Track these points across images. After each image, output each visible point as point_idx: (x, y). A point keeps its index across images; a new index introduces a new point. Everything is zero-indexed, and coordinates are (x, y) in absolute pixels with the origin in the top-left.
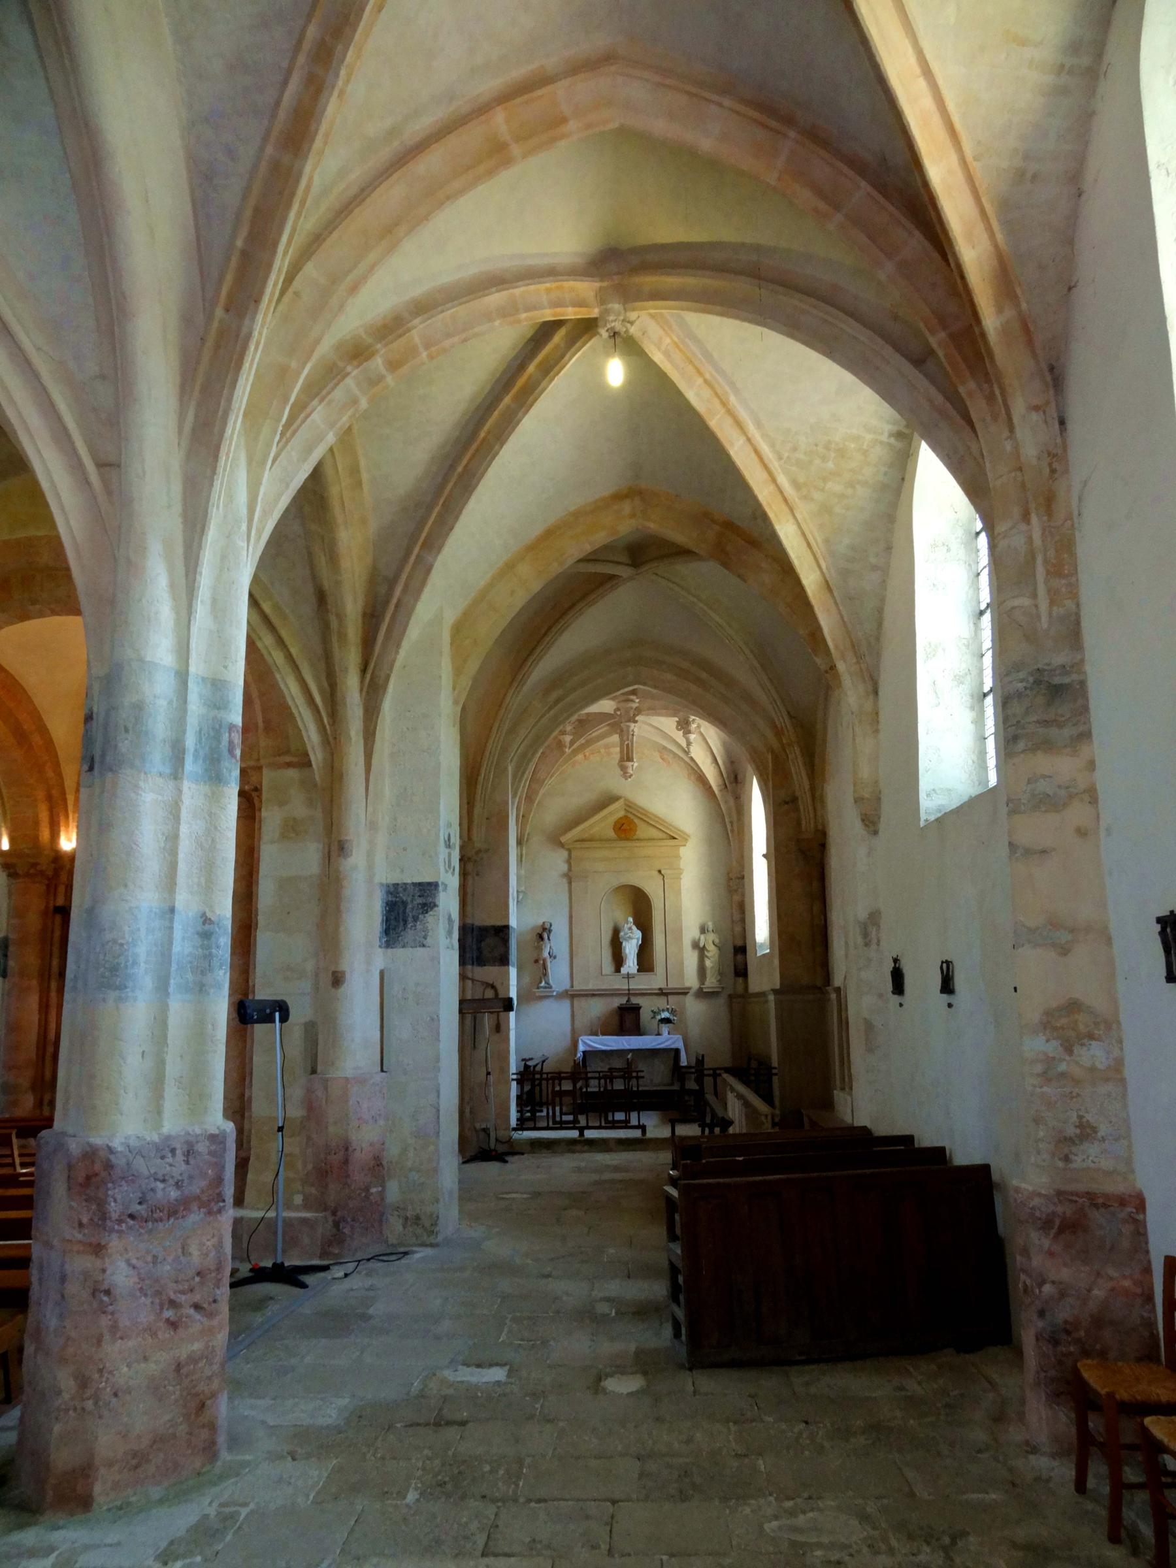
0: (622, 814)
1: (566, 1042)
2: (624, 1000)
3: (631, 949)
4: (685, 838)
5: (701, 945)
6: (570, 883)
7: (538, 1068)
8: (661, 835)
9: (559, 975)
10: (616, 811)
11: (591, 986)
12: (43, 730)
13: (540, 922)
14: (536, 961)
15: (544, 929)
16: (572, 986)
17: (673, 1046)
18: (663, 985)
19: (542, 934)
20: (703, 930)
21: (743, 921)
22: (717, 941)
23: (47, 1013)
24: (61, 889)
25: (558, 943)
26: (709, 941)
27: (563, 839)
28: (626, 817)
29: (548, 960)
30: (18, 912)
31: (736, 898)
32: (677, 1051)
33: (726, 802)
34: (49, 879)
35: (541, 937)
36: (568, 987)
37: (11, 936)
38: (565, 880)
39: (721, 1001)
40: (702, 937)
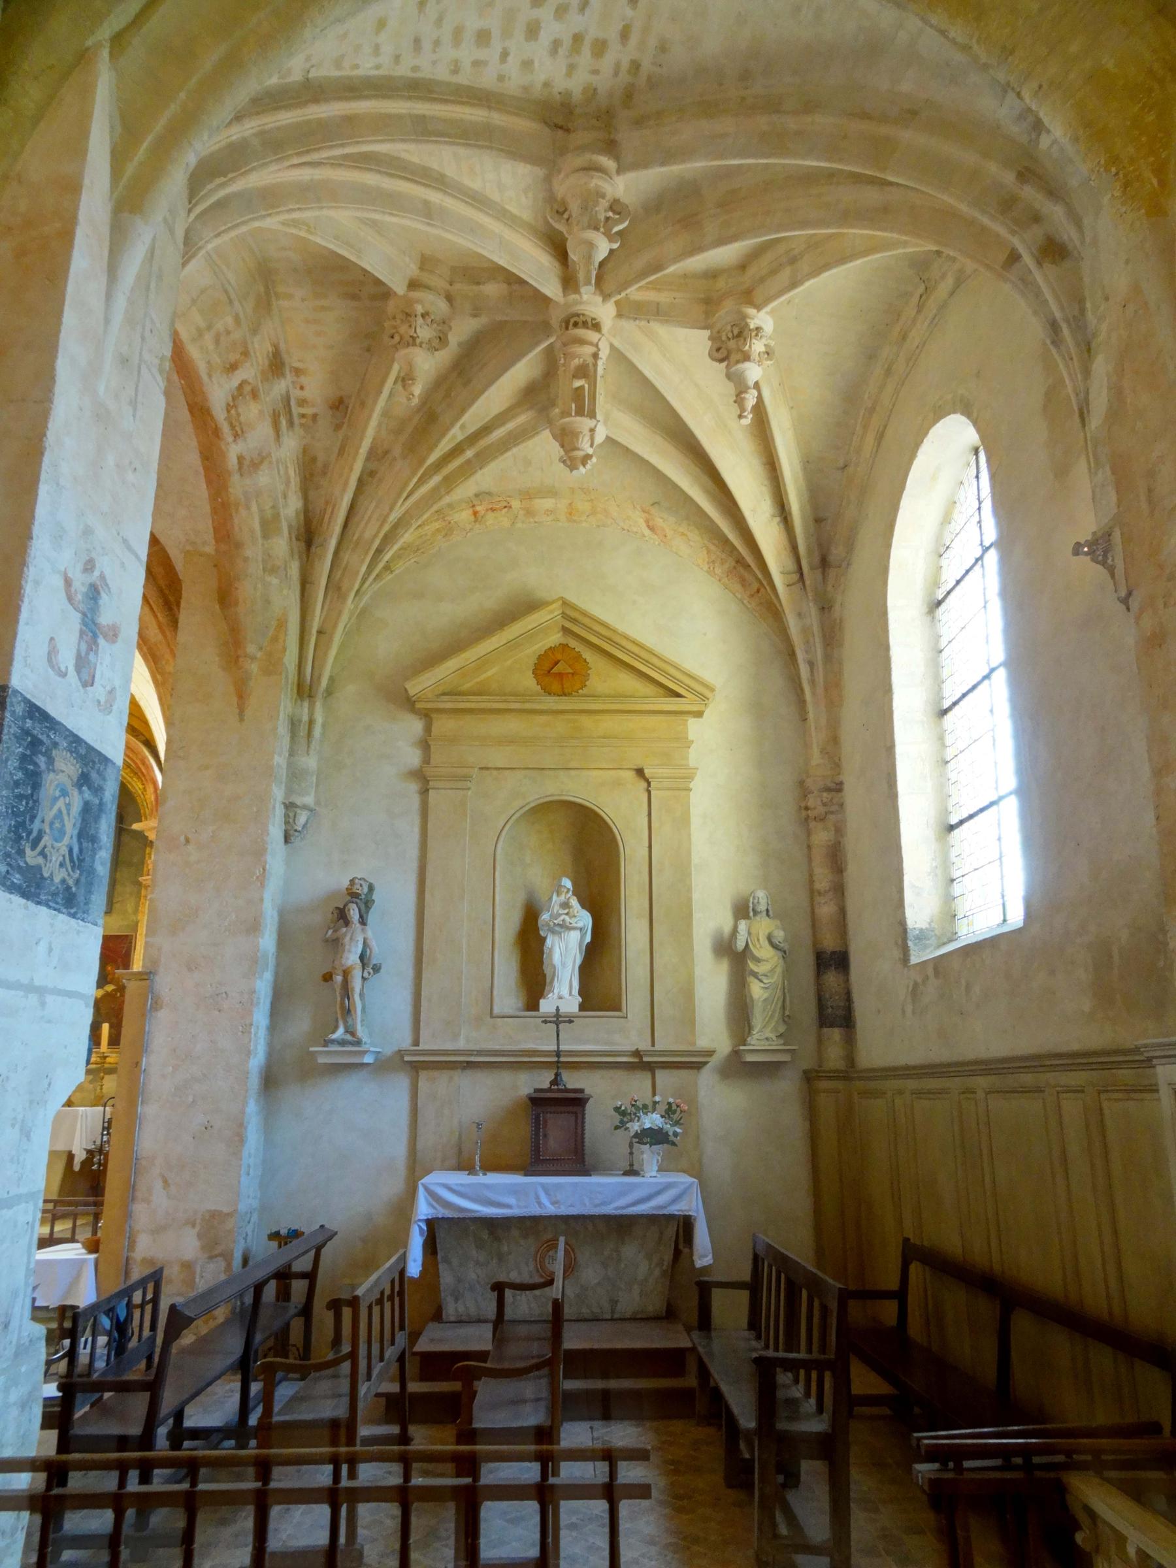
0: (555, 638)
1: (393, 1186)
2: (544, 1080)
3: (565, 952)
4: (703, 693)
5: (740, 945)
6: (424, 792)
7: (303, 1264)
8: (650, 689)
9: (383, 1014)
10: (541, 632)
11: (466, 1040)
13: (346, 883)
14: (328, 977)
15: (353, 895)
16: (416, 1042)
17: (675, 1209)
18: (644, 1045)
19: (350, 906)
20: (743, 910)
21: (839, 889)
22: (779, 935)
25: (388, 932)
26: (759, 933)
27: (414, 687)
28: (564, 646)
29: (357, 974)
31: (822, 837)
32: (686, 1225)
33: (800, 615)
35: (342, 916)
36: (406, 1043)
38: (413, 787)
39: (788, 1086)
40: (743, 925)
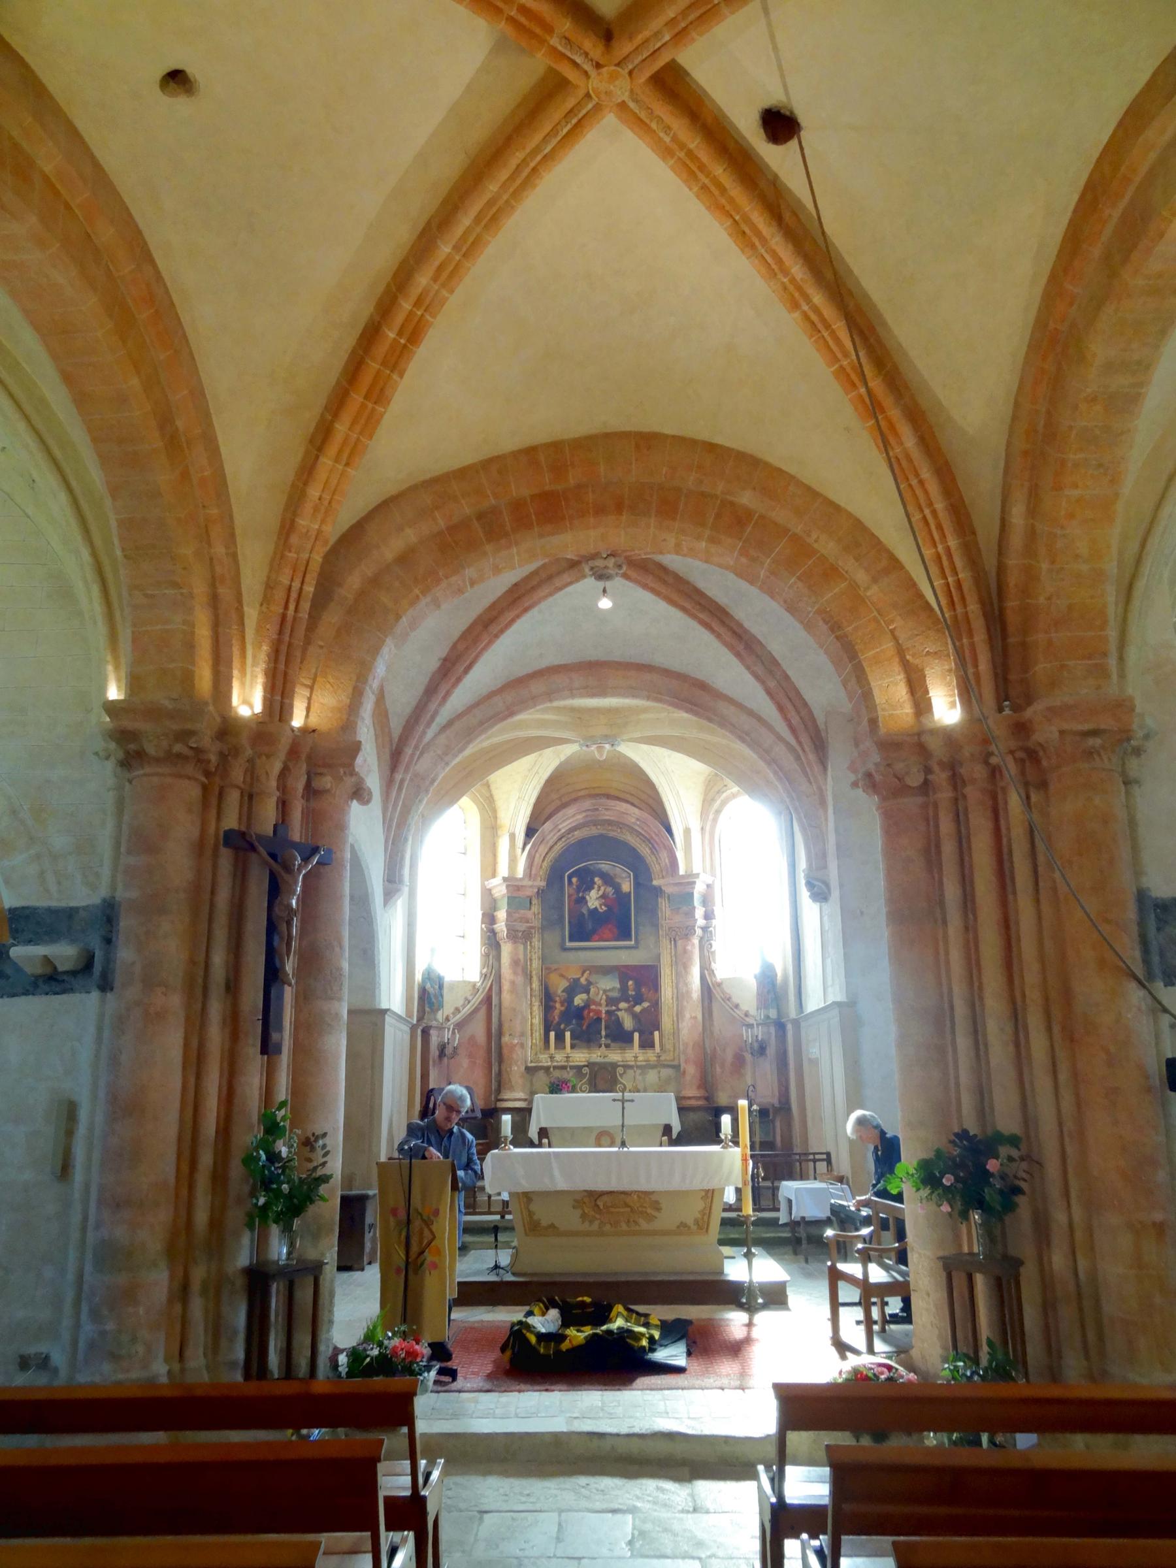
23: (198, 1077)
24: (233, 798)
30: (142, 842)
34: (207, 774)
37: (121, 894)
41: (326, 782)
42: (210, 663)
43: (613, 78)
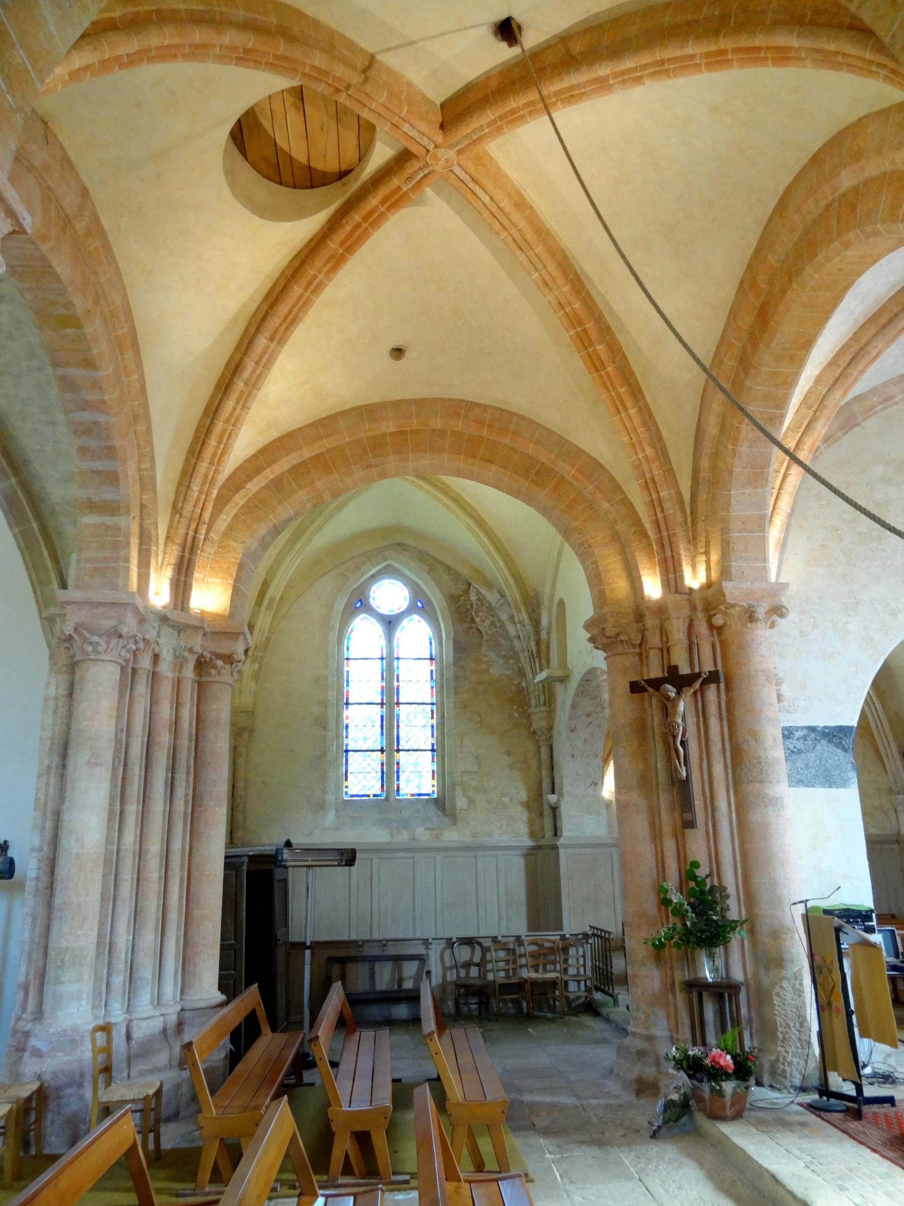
12: (572, 453)
41: (718, 620)
42: (624, 575)
43: (436, 158)
